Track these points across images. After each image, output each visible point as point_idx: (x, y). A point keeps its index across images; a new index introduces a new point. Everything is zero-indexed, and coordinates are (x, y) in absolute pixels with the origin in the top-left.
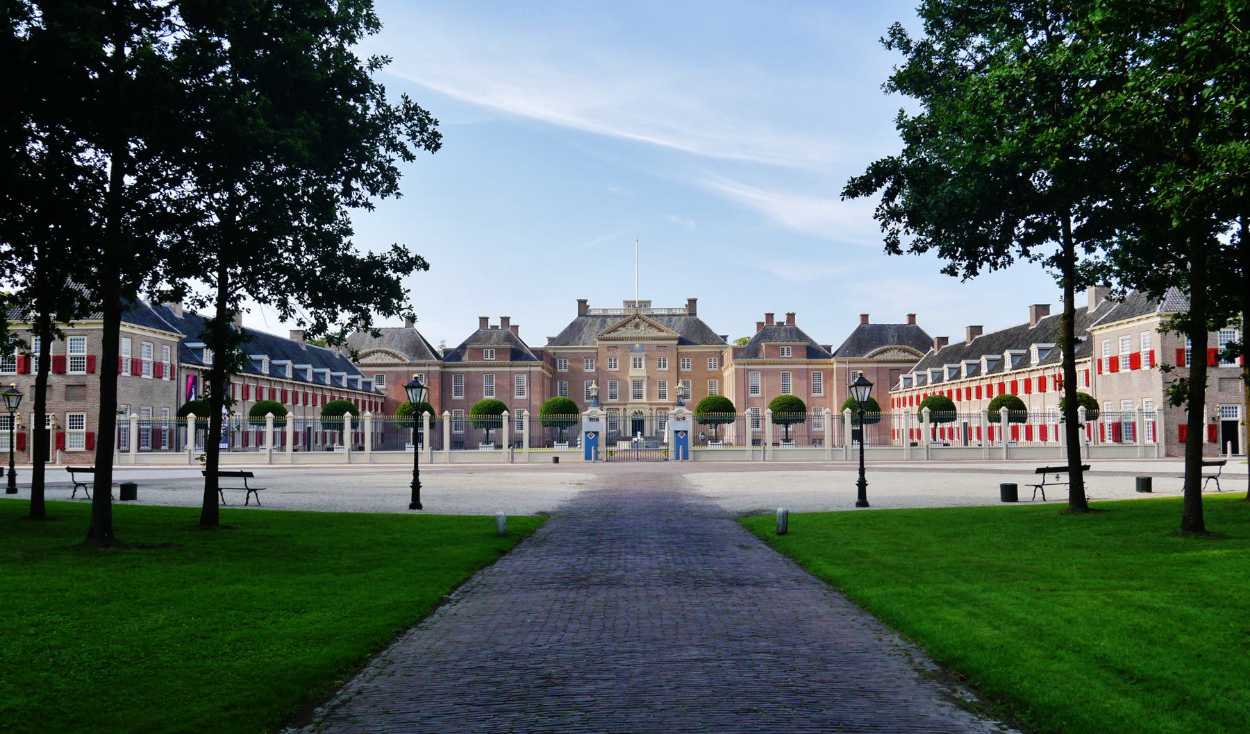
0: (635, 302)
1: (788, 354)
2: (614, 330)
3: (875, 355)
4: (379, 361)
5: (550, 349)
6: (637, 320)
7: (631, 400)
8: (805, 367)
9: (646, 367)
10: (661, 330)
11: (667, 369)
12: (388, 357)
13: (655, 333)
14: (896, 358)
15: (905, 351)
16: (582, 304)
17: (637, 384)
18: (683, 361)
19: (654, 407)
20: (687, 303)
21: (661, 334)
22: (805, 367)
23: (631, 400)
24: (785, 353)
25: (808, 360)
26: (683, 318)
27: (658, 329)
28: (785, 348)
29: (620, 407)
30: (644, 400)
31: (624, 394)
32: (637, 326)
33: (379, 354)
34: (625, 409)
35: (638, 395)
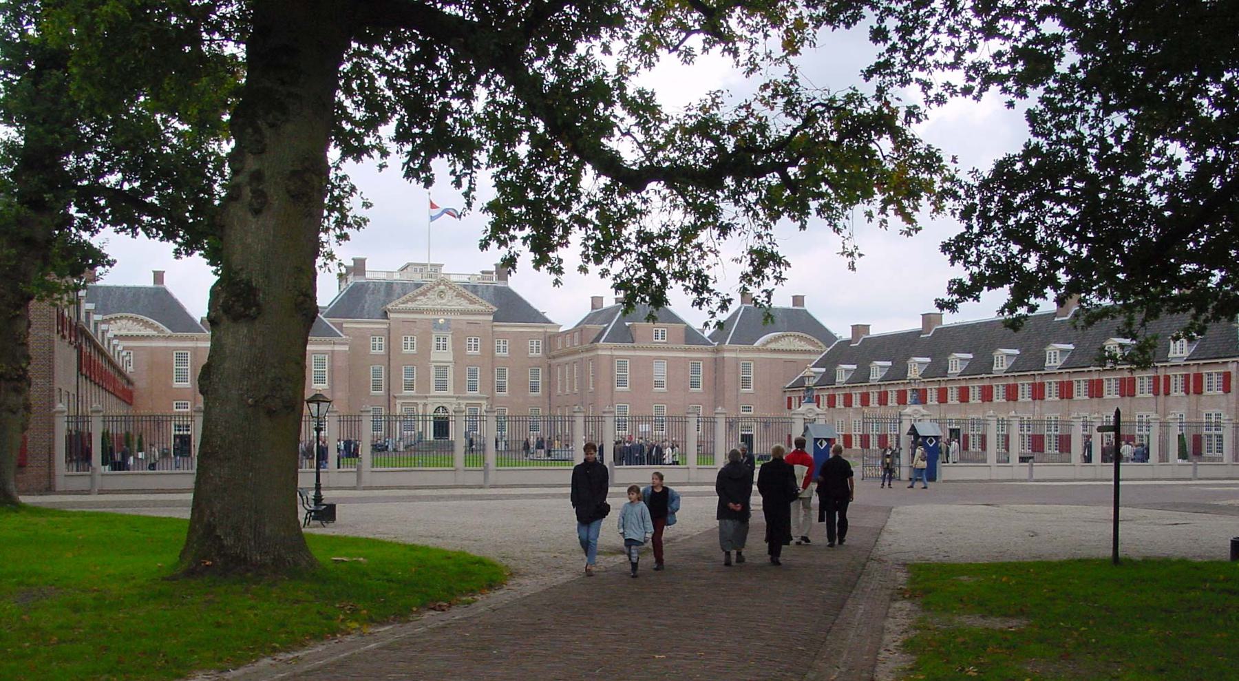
0: (426, 265)
2: (413, 300)
3: (768, 343)
4: (124, 332)
6: (442, 287)
7: (433, 392)
8: (683, 355)
10: (472, 302)
11: (478, 352)
12: (138, 327)
13: (465, 305)
14: (792, 348)
15: (801, 339)
17: (441, 370)
18: (499, 342)
21: (471, 307)
22: (683, 355)
23: (433, 392)
24: (660, 337)
25: (687, 346)
28: (660, 330)
29: (418, 402)
30: (450, 391)
31: (424, 384)
32: (441, 294)
33: (124, 322)
34: (425, 405)
35: (441, 386)
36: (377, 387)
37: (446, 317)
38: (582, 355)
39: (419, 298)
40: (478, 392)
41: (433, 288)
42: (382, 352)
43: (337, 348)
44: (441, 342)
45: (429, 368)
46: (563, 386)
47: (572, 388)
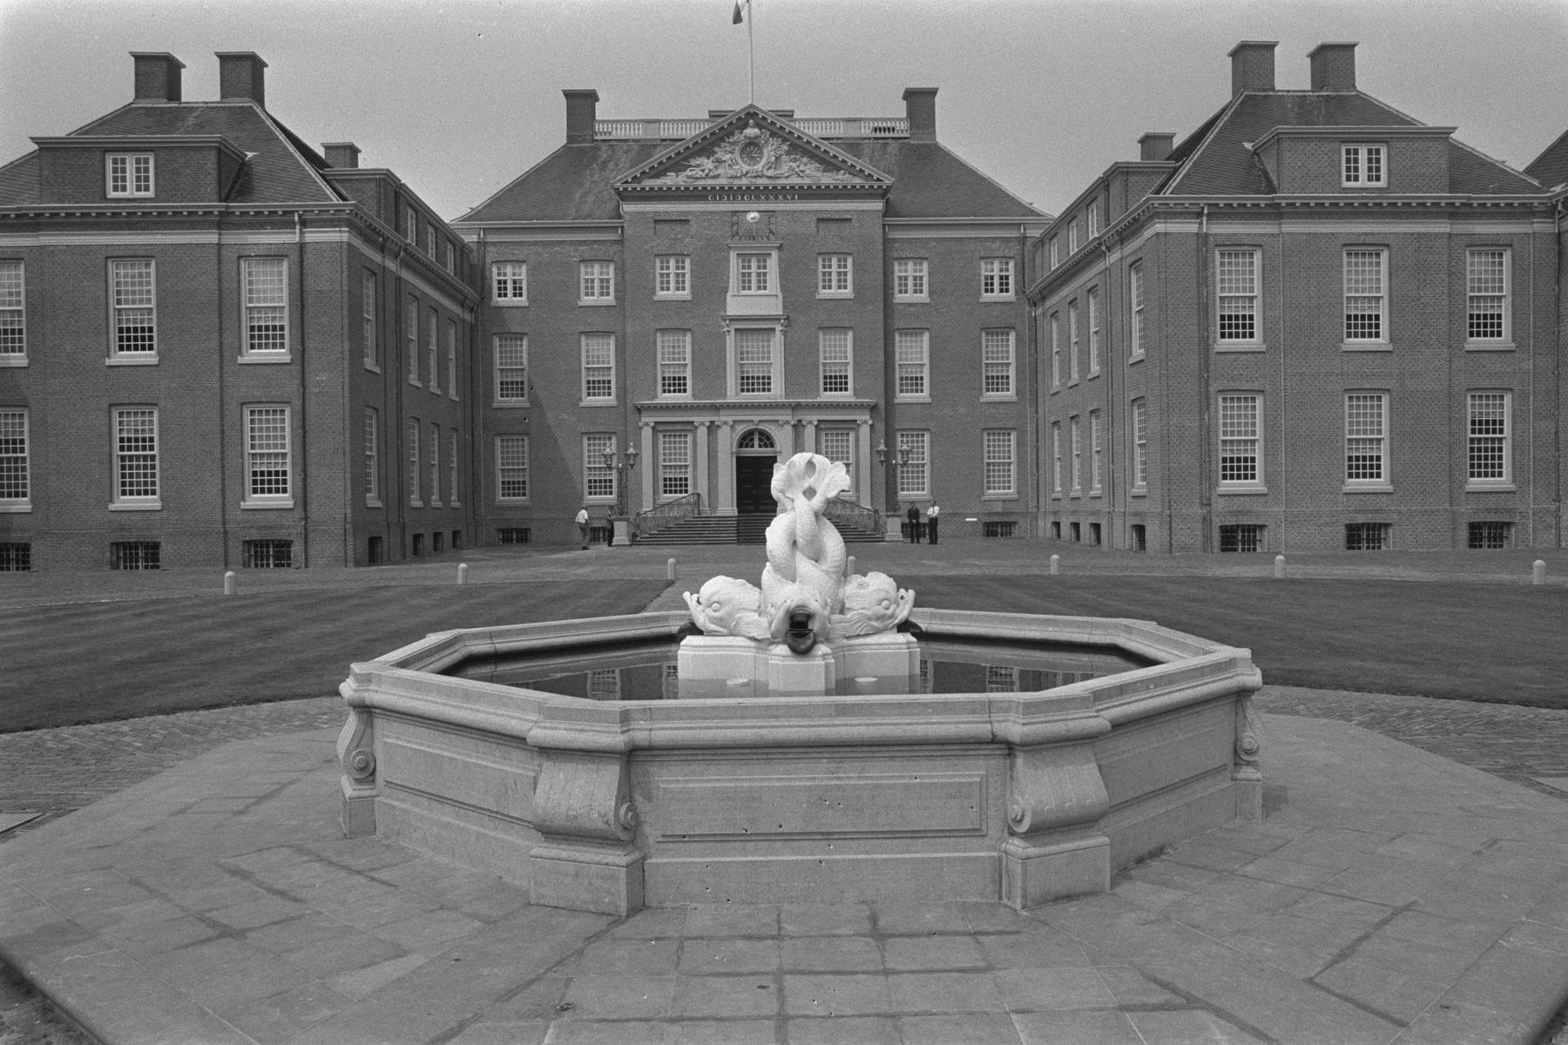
1: (1374, 174)
2: (677, 163)
5: (470, 230)
6: (751, 131)
9: (783, 288)
10: (829, 164)
11: (848, 293)
13: (811, 174)
16: (581, 103)
19: (815, 418)
20: (901, 109)
21: (827, 179)
24: (1363, 172)
26: (893, 147)
27: (821, 161)
29: (696, 419)
34: (712, 428)
36: (595, 387)
37: (764, 207)
38: (1114, 257)
39: (693, 162)
40: (850, 392)
41: (732, 134)
42: (610, 299)
43: (314, 236)
44: (754, 269)
45: (722, 336)
46: (1065, 372)
47: (1084, 365)
